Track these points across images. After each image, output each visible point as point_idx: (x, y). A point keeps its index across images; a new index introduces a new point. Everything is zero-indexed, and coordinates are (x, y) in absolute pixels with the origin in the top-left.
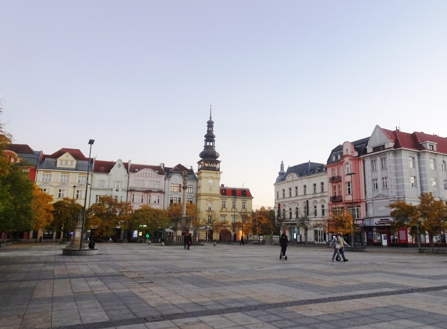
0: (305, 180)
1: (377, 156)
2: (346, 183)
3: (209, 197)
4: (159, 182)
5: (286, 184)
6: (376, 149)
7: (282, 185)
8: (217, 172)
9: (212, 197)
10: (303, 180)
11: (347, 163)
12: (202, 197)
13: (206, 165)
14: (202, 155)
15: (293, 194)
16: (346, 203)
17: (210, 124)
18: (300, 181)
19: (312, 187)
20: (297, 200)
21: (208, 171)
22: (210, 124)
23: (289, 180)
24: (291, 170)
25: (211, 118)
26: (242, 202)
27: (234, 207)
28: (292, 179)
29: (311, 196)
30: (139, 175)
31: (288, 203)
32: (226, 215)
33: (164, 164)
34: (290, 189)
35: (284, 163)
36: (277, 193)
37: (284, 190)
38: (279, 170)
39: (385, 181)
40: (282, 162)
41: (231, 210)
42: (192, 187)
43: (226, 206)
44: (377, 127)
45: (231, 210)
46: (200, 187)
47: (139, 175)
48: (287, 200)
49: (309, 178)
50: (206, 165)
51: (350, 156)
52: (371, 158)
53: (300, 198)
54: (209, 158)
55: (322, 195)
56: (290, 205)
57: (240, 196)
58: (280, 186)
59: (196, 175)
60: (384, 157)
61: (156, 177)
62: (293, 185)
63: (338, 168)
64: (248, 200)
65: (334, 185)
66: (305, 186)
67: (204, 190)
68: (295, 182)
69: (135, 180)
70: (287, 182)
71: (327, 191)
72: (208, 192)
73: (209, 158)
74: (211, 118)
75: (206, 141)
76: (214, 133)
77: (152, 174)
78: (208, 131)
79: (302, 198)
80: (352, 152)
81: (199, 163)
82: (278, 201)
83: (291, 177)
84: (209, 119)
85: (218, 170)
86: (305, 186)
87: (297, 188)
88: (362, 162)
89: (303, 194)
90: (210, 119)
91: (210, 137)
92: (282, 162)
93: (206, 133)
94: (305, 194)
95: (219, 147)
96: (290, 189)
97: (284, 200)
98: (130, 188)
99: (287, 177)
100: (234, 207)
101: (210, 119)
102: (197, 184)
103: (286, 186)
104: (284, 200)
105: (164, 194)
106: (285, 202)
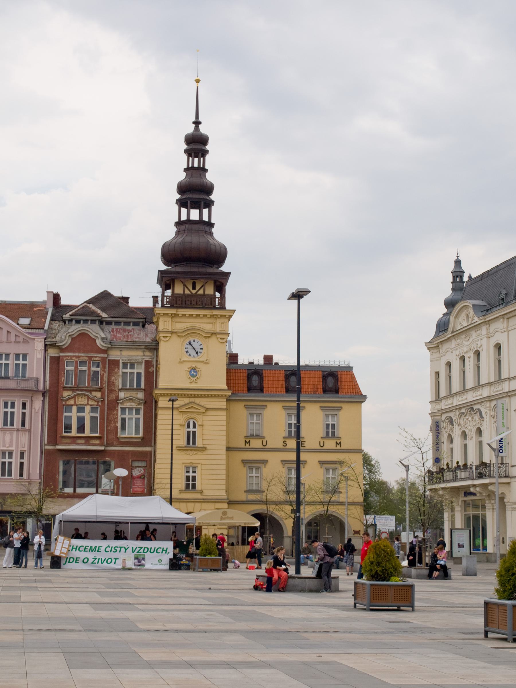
0: (499, 325)
3: (187, 400)
5: (453, 343)
9: (197, 401)
10: (494, 326)
14: (169, 255)
17: (196, 145)
18: (484, 330)
20: (481, 402)
21: (181, 312)
22: (196, 145)
25: (197, 123)
28: (465, 324)
32: (265, 462)
33: (56, 298)
40: (458, 263)
41: (280, 445)
45: (280, 445)
50: (179, 289)
53: (485, 392)
54: (195, 266)
61: (12, 338)
64: (345, 406)
66: (498, 347)
67: (171, 375)
70: (457, 334)
73: (195, 266)
74: (197, 123)
75: (182, 203)
76: (210, 177)
82: (438, 407)
83: (463, 317)
84: (190, 129)
86: (498, 347)
87: (477, 354)
90: (197, 128)
91: (195, 192)
92: (458, 263)
93: (182, 176)
95: (226, 225)
101: (197, 128)
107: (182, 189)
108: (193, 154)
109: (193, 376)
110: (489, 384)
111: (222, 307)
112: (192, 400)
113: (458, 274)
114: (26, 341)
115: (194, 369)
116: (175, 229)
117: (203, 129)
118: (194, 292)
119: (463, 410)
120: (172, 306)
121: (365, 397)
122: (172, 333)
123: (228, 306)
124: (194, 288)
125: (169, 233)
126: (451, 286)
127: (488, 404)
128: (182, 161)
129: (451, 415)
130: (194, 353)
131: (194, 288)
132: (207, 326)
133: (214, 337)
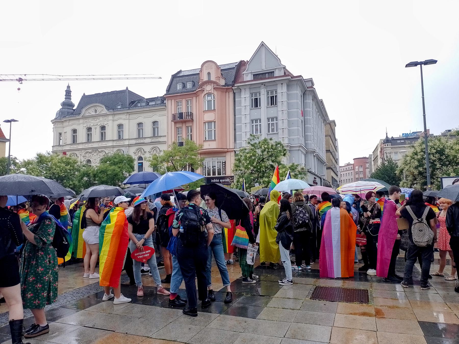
0: (123, 116)
1: (263, 86)
5: (81, 121)
6: (256, 76)
7: (71, 123)
10: (116, 117)
11: (209, 94)
15: (96, 136)
18: (110, 118)
19: (134, 129)
23: (87, 115)
24: (87, 100)
29: (133, 142)
31: (83, 153)
34: (89, 129)
35: (71, 89)
36: (58, 134)
37: (75, 131)
38: (63, 99)
39: (271, 122)
40: (69, 87)
44: (263, 45)
48: (81, 147)
49: (129, 114)
51: (214, 83)
52: (250, 88)
55: (155, 140)
56: (87, 155)
58: (66, 124)
60: (272, 88)
62: (96, 124)
63: (187, 101)
65: (178, 125)
68: (101, 119)
70: (84, 118)
71: (166, 134)
79: (115, 144)
80: (218, 78)
82: (60, 148)
86: (120, 126)
87: (103, 128)
88: (231, 95)
89: (116, 138)
92: (69, 87)
94: (120, 138)
96: (89, 129)
97: (75, 147)
99: (84, 110)
104: (90, 145)
106: (78, 150)
110: (113, 141)
119: (90, 151)
126: (64, 97)
127: (112, 149)
129: (77, 152)
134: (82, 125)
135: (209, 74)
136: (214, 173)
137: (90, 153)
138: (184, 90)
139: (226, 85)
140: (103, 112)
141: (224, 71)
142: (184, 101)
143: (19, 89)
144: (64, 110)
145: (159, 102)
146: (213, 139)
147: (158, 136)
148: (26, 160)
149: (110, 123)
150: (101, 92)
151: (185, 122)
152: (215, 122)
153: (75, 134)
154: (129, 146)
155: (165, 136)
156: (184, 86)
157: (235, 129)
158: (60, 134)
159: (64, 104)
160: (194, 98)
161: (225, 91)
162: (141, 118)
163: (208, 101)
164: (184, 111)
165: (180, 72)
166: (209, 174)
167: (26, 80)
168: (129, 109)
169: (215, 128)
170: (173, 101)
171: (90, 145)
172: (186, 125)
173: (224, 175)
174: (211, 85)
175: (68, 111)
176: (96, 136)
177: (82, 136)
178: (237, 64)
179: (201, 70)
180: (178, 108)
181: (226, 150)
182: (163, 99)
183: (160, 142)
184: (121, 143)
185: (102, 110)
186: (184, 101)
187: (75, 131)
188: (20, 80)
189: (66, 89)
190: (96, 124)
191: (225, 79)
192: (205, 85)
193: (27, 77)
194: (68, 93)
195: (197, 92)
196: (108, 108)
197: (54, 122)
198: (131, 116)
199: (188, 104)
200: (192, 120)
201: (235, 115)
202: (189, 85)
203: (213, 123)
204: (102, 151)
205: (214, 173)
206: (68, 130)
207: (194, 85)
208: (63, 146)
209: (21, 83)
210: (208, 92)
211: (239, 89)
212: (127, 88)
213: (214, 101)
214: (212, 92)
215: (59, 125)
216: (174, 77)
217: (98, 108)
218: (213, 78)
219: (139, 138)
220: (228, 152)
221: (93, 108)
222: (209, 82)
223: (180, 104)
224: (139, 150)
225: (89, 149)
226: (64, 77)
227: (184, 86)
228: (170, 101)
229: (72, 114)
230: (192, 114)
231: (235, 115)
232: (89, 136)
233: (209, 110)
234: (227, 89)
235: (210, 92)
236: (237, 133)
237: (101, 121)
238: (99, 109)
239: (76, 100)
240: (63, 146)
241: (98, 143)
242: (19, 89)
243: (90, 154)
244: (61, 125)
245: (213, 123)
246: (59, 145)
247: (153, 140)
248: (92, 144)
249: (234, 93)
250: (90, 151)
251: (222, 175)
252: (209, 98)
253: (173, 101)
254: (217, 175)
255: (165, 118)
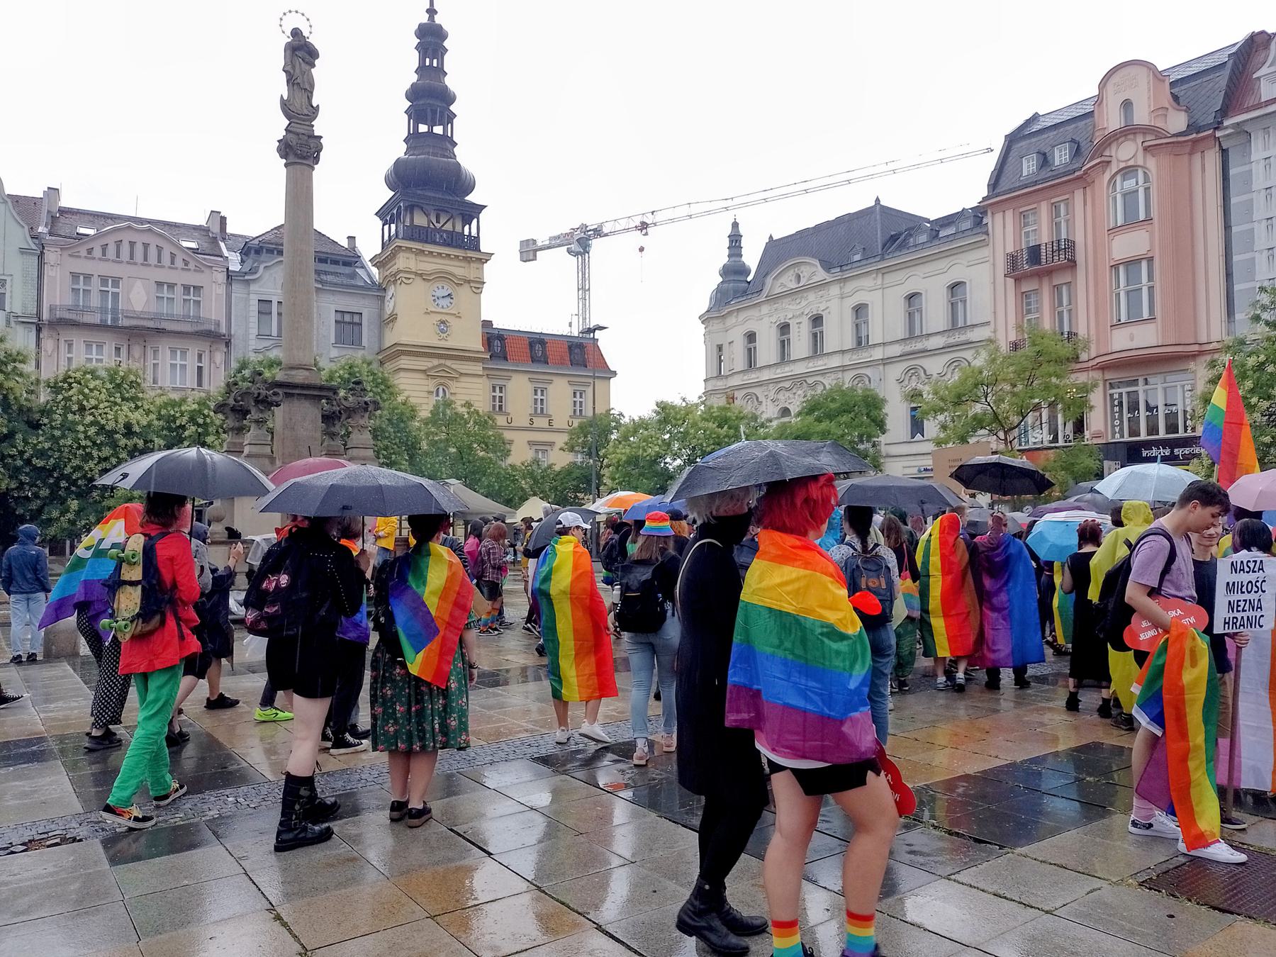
0: (868, 282)
2: (1115, 267)
3: (436, 362)
4: (198, 289)
5: (765, 309)
7: (742, 316)
8: (470, 254)
9: (449, 363)
10: (850, 286)
12: (404, 362)
13: (420, 220)
14: (401, 178)
15: (800, 343)
16: (1103, 368)
17: (431, 40)
18: (835, 290)
22: (431, 40)
24: (778, 251)
25: (432, 12)
26: (570, 390)
27: (539, 410)
28: (793, 285)
29: (896, 350)
30: (97, 252)
33: (223, 220)
34: (784, 328)
35: (742, 230)
36: (715, 349)
37: (751, 337)
38: (723, 258)
42: (356, 319)
43: (509, 407)
46: (393, 318)
47: (97, 252)
48: (765, 375)
50: (420, 220)
51: (1145, 130)
54: (432, 195)
56: (781, 396)
57: (561, 363)
58: (731, 321)
59: (375, 271)
61: (179, 263)
62: (797, 312)
63: (1055, 207)
66: (860, 310)
68: (811, 296)
69: (75, 276)
71: (990, 318)
72: (435, 342)
73: (432, 195)
74: (432, 12)
75: (416, 114)
76: (450, 82)
77: (160, 249)
78: (421, 70)
80: (1161, 111)
81: (386, 215)
82: (720, 384)
83: (783, 280)
84: (424, 18)
85: (474, 243)
86: (860, 310)
87: (817, 320)
88: (1212, 159)
89: (849, 343)
90: (431, 18)
96: (784, 328)
97: (753, 377)
98: (52, 309)
99: (769, 280)
100: (539, 410)
101: (431, 18)
102: (382, 308)
103: (764, 322)
105: (228, 344)
106: (760, 384)
107: (414, 94)
108: (430, 51)
109: (443, 331)
110: (843, 352)
111: (477, 248)
112: (442, 361)
113: (735, 241)
114: (198, 270)
115: (443, 322)
116: (405, 146)
117: (438, 19)
118: (438, 226)
119: (787, 384)
120: (411, 239)
121: (615, 373)
122: (416, 274)
123: (483, 248)
124: (438, 222)
125: (400, 150)
126: (727, 252)
128: (413, 59)
129: (757, 391)
130: (448, 300)
131: (438, 222)
132: (459, 270)
133: (467, 285)
134: (766, 320)
135: (1127, 105)
136: (1153, 429)
137: (787, 390)
138: (1045, 173)
139: (1193, 127)
140: (815, 279)
141: (1182, 86)
142: (1044, 208)
143: (642, 249)
144: (725, 285)
145: (967, 225)
146: (1146, 315)
147: (966, 327)
148: (636, 419)
149: (834, 305)
150: (812, 225)
151: (1049, 272)
152: (1150, 260)
153: (752, 346)
154: (886, 362)
155: (988, 323)
156: (1048, 160)
157: (1229, 275)
158: (720, 348)
159: (726, 271)
160: (1079, 195)
161: (1187, 149)
162: (914, 280)
163: (1124, 195)
164: (1044, 237)
165: (1035, 117)
166: (1134, 432)
167: (655, 224)
168: (883, 259)
169: (1150, 278)
170: (1009, 214)
171: (787, 370)
172: (1050, 281)
173: (1190, 433)
174: (1134, 140)
175: (737, 287)
176: (800, 343)
177: (767, 350)
178: (1234, 50)
179: (1099, 100)
180: (1027, 234)
181: (1196, 348)
182: (978, 216)
183: (925, 352)
184: (864, 356)
185: (814, 271)
186: (1044, 208)
187: (751, 337)
188: (644, 226)
189: (729, 230)
190: (797, 312)
191: (1188, 110)
192: (1114, 146)
193: (659, 217)
194: (735, 241)
195: (1086, 173)
196: (827, 266)
197: (706, 319)
198: (890, 278)
199: (1058, 215)
200: (1072, 264)
201: (1227, 227)
202: (1061, 157)
203: (1144, 264)
204: (816, 383)
205: (1153, 429)
206: (737, 336)
207: (1077, 152)
208: (727, 377)
209: (646, 234)
210: (1122, 165)
211: (1243, 132)
212: (878, 200)
213: (1147, 189)
214: (1140, 162)
215: (717, 326)
216: (1013, 139)
217: (803, 268)
218: (1141, 116)
219: (912, 337)
220: (1201, 353)
221: (791, 272)
222: (1129, 131)
223: (1031, 219)
224: (912, 372)
225: (786, 379)
226: (736, 201)
227: (1045, 160)
228: (999, 217)
229: (744, 293)
230: (1071, 245)
231: (1227, 227)
232: (784, 345)
233: (1131, 223)
234: (1195, 142)
235: (1131, 163)
236: (1237, 287)
237: (813, 303)
238: (805, 272)
239: (752, 257)
240: (727, 377)
241: (804, 364)
242: (642, 249)
243: (787, 394)
244: (721, 326)
245: (1144, 264)
246: (719, 376)
247: (951, 340)
248: (792, 367)
249: (1224, 152)
250: (787, 384)
251: (1181, 434)
252: (1130, 184)
253: (1009, 214)
254: (1162, 434)
255: (987, 267)
